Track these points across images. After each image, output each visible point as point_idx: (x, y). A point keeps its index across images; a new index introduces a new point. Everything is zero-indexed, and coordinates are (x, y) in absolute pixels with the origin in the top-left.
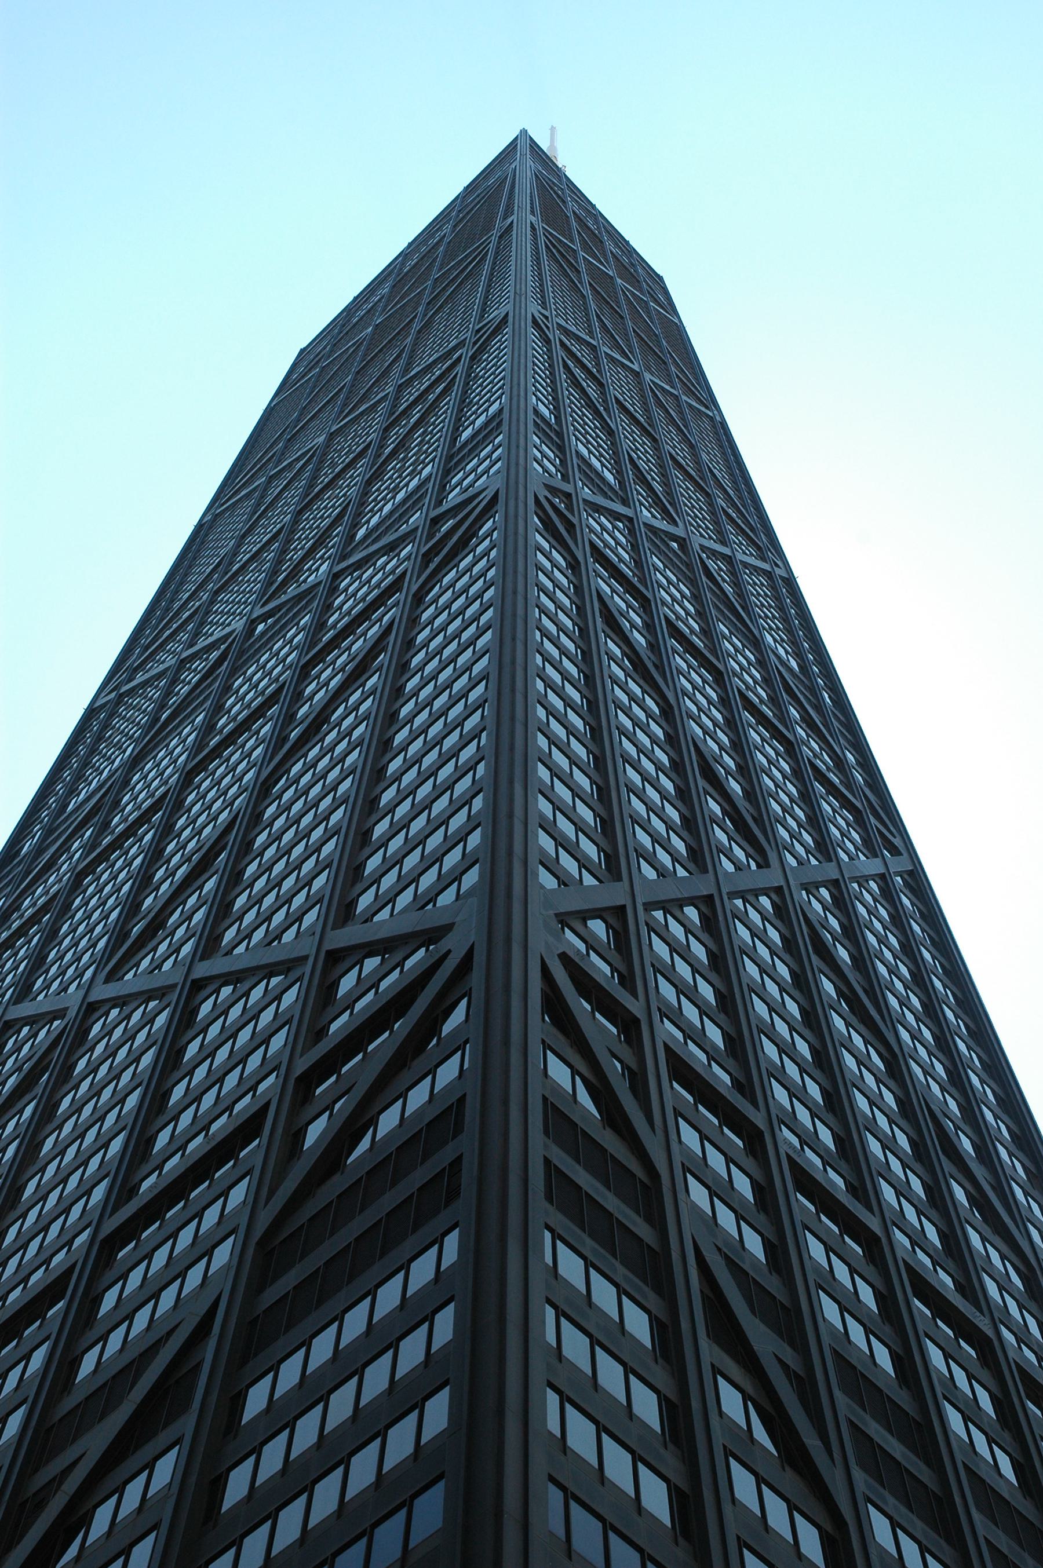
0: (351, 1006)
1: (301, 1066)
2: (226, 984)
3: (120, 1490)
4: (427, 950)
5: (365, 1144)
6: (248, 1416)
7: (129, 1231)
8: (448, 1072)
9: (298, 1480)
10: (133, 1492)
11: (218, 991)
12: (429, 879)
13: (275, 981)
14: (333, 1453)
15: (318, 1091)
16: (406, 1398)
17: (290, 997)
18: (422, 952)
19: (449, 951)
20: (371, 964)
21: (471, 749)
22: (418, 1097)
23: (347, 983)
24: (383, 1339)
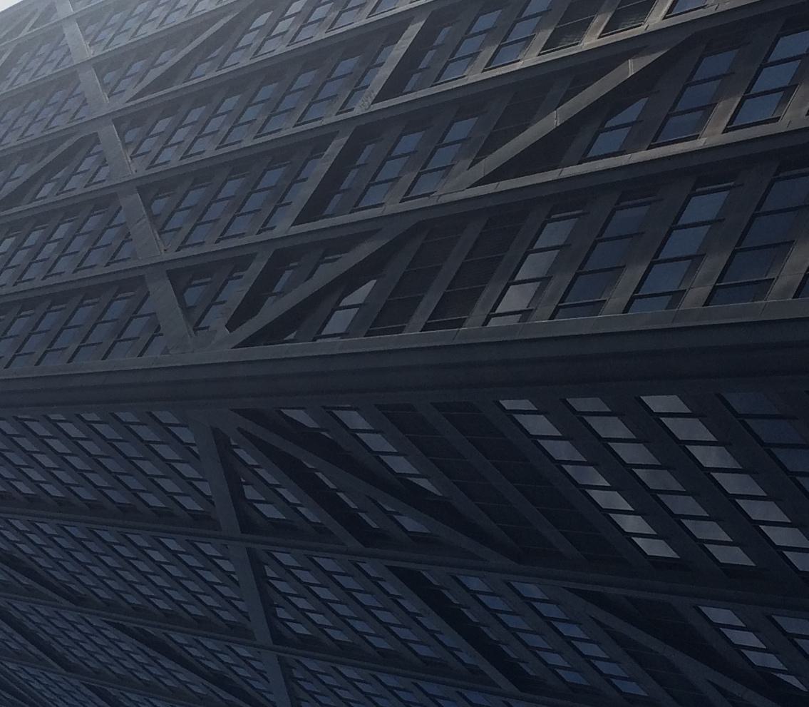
0: (294, 507)
1: (353, 544)
2: (275, 614)
3: (739, 648)
4: (237, 447)
5: (424, 483)
6: (671, 554)
7: (511, 669)
8: (355, 420)
9: (725, 509)
10: (739, 637)
11: (282, 621)
12: (167, 452)
13: (270, 573)
14: (701, 482)
15: (374, 526)
16: (651, 430)
17: (286, 559)
18: (239, 452)
19: (239, 429)
20: (250, 492)
21: (34, 426)
22: (377, 442)
23: (271, 511)
24: (600, 453)
